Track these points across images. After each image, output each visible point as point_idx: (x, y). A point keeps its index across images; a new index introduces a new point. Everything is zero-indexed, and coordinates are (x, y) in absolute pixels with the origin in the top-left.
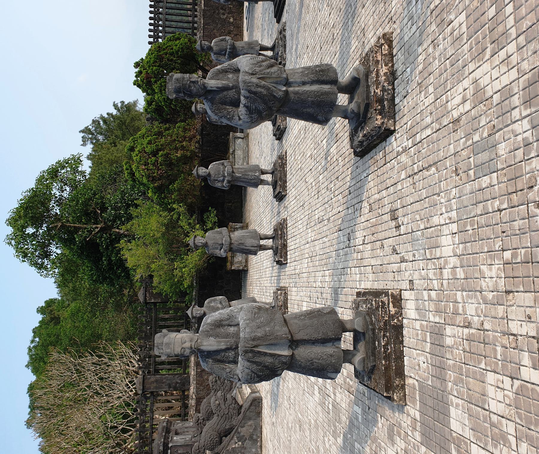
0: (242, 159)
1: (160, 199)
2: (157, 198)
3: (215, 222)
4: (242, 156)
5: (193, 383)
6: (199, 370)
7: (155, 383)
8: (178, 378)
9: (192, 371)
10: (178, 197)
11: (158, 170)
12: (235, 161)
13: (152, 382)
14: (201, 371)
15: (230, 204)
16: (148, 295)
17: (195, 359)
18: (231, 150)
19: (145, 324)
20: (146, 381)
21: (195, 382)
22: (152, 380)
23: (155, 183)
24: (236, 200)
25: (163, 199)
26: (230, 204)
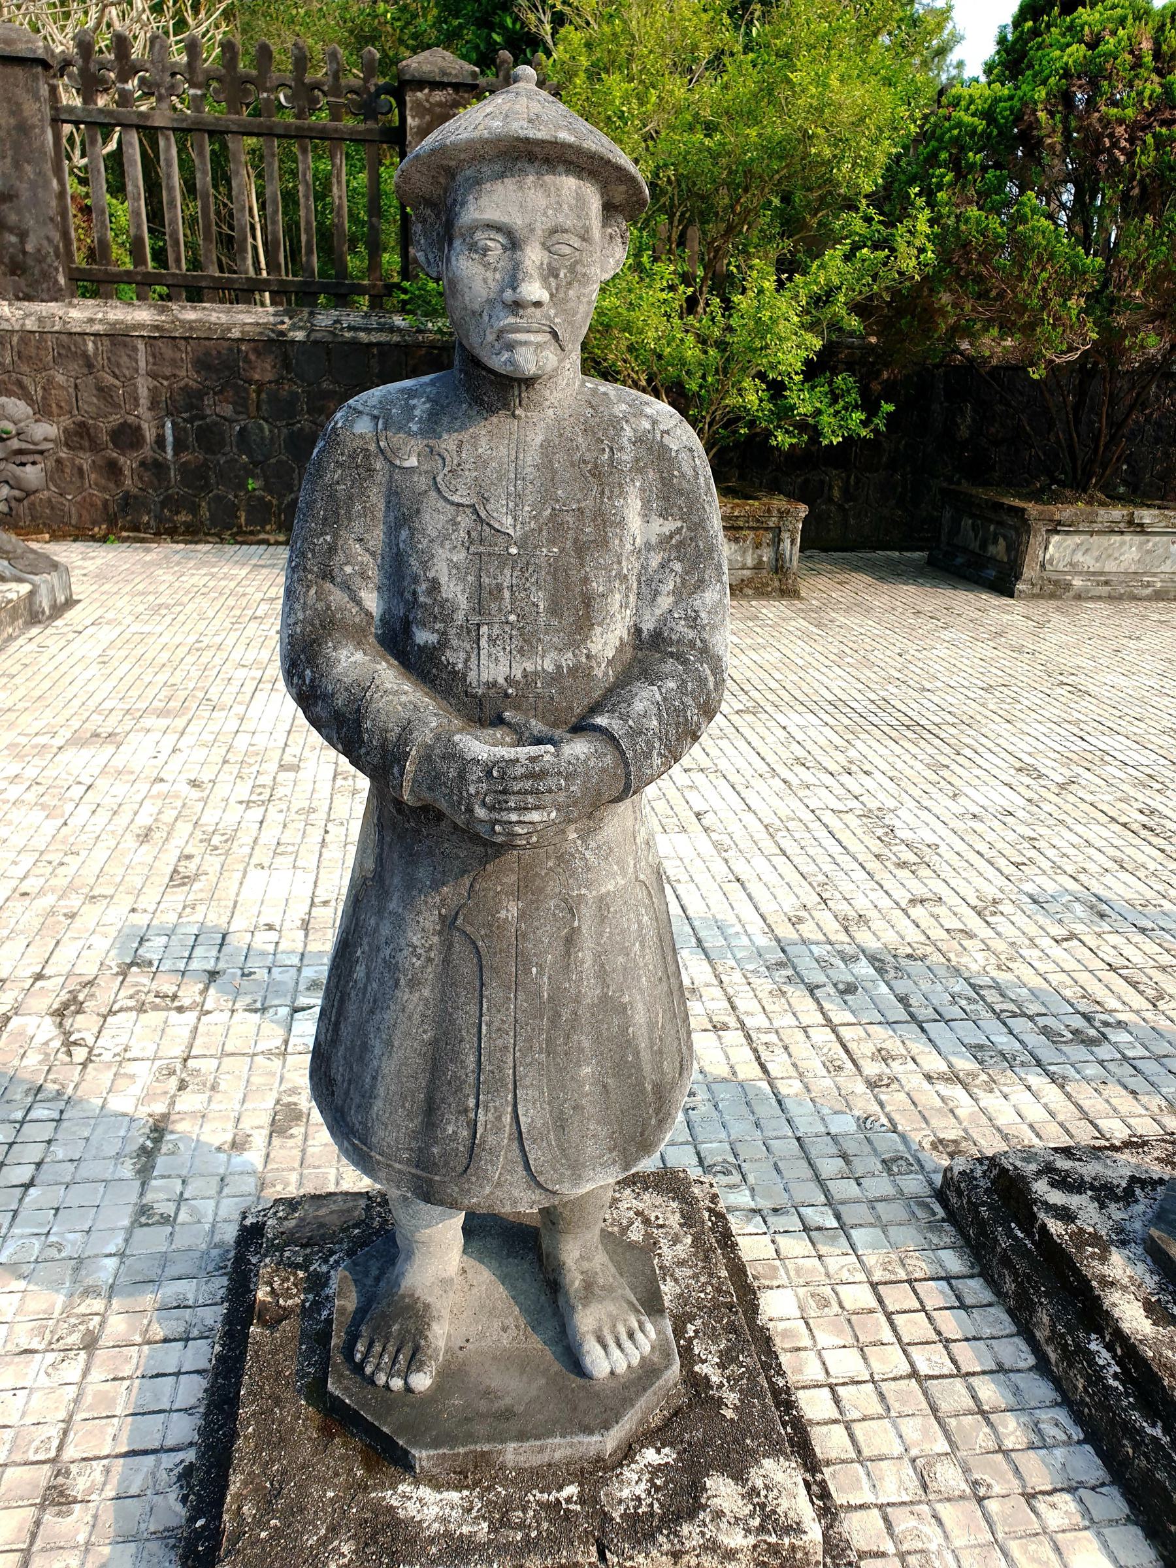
0: (1097, 567)
1: (956, 141)
2: (959, 124)
3: (815, 432)
4: (1110, 566)
5: (27, 316)
6: (90, 346)
7: (12, 121)
8: (48, 239)
9: (87, 314)
10: (976, 240)
11: (1136, 130)
12: (1091, 533)
13: (18, 104)
14: (85, 355)
15: (836, 493)
16: (439, 96)
17: (142, 326)
18: (1146, 516)
19: (299, 79)
20: (19, 72)
21: (31, 325)
22: (26, 107)
23: (1052, 114)
24: (852, 522)
25: (957, 165)
26: (836, 493)
